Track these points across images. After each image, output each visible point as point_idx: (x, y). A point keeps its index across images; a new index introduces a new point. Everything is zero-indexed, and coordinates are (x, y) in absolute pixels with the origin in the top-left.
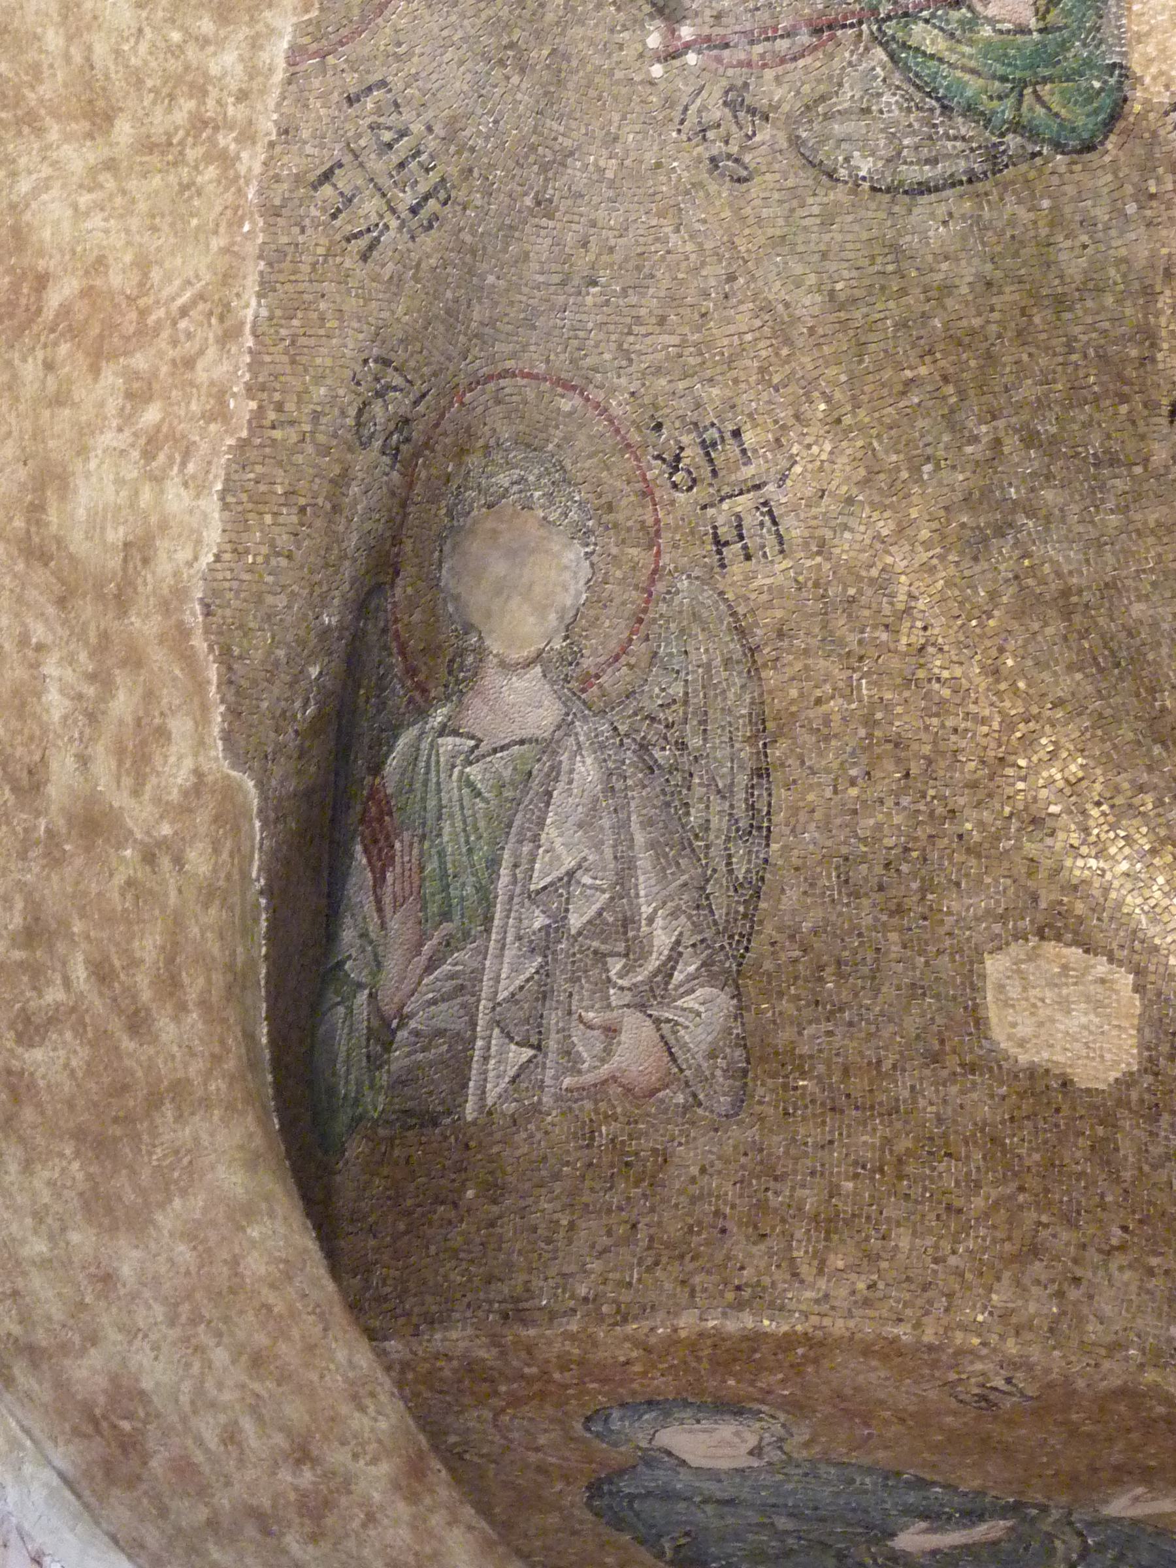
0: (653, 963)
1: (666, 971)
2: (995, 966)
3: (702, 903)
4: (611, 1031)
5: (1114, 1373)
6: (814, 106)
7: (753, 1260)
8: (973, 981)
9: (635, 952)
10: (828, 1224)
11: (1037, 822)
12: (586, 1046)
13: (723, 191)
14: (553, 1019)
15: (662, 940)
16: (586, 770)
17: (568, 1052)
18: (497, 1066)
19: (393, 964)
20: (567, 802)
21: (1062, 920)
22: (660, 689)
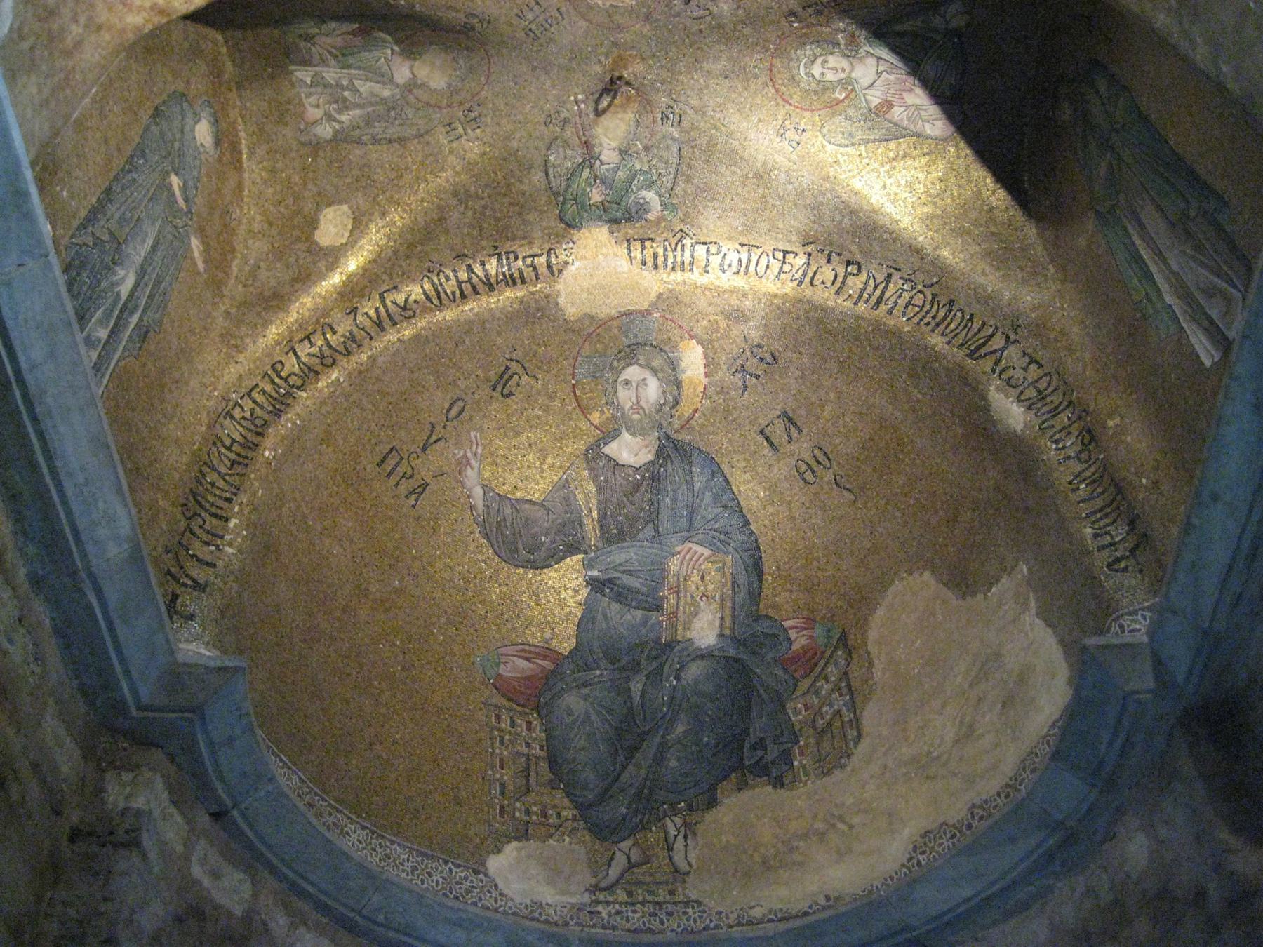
0: (337, 117)
1: (335, 120)
2: (345, 207)
3: (355, 128)
4: (318, 106)
5: (239, 247)
6: (566, 144)
7: (261, 151)
8: (340, 202)
9: (339, 111)
10: (273, 171)
11: (383, 215)
12: (313, 100)
13: (542, 118)
14: (319, 90)
15: (344, 118)
16: (386, 93)
17: (311, 94)
18: (303, 75)
19: (329, 40)
20: (377, 88)
21: (359, 224)
22: (410, 112)
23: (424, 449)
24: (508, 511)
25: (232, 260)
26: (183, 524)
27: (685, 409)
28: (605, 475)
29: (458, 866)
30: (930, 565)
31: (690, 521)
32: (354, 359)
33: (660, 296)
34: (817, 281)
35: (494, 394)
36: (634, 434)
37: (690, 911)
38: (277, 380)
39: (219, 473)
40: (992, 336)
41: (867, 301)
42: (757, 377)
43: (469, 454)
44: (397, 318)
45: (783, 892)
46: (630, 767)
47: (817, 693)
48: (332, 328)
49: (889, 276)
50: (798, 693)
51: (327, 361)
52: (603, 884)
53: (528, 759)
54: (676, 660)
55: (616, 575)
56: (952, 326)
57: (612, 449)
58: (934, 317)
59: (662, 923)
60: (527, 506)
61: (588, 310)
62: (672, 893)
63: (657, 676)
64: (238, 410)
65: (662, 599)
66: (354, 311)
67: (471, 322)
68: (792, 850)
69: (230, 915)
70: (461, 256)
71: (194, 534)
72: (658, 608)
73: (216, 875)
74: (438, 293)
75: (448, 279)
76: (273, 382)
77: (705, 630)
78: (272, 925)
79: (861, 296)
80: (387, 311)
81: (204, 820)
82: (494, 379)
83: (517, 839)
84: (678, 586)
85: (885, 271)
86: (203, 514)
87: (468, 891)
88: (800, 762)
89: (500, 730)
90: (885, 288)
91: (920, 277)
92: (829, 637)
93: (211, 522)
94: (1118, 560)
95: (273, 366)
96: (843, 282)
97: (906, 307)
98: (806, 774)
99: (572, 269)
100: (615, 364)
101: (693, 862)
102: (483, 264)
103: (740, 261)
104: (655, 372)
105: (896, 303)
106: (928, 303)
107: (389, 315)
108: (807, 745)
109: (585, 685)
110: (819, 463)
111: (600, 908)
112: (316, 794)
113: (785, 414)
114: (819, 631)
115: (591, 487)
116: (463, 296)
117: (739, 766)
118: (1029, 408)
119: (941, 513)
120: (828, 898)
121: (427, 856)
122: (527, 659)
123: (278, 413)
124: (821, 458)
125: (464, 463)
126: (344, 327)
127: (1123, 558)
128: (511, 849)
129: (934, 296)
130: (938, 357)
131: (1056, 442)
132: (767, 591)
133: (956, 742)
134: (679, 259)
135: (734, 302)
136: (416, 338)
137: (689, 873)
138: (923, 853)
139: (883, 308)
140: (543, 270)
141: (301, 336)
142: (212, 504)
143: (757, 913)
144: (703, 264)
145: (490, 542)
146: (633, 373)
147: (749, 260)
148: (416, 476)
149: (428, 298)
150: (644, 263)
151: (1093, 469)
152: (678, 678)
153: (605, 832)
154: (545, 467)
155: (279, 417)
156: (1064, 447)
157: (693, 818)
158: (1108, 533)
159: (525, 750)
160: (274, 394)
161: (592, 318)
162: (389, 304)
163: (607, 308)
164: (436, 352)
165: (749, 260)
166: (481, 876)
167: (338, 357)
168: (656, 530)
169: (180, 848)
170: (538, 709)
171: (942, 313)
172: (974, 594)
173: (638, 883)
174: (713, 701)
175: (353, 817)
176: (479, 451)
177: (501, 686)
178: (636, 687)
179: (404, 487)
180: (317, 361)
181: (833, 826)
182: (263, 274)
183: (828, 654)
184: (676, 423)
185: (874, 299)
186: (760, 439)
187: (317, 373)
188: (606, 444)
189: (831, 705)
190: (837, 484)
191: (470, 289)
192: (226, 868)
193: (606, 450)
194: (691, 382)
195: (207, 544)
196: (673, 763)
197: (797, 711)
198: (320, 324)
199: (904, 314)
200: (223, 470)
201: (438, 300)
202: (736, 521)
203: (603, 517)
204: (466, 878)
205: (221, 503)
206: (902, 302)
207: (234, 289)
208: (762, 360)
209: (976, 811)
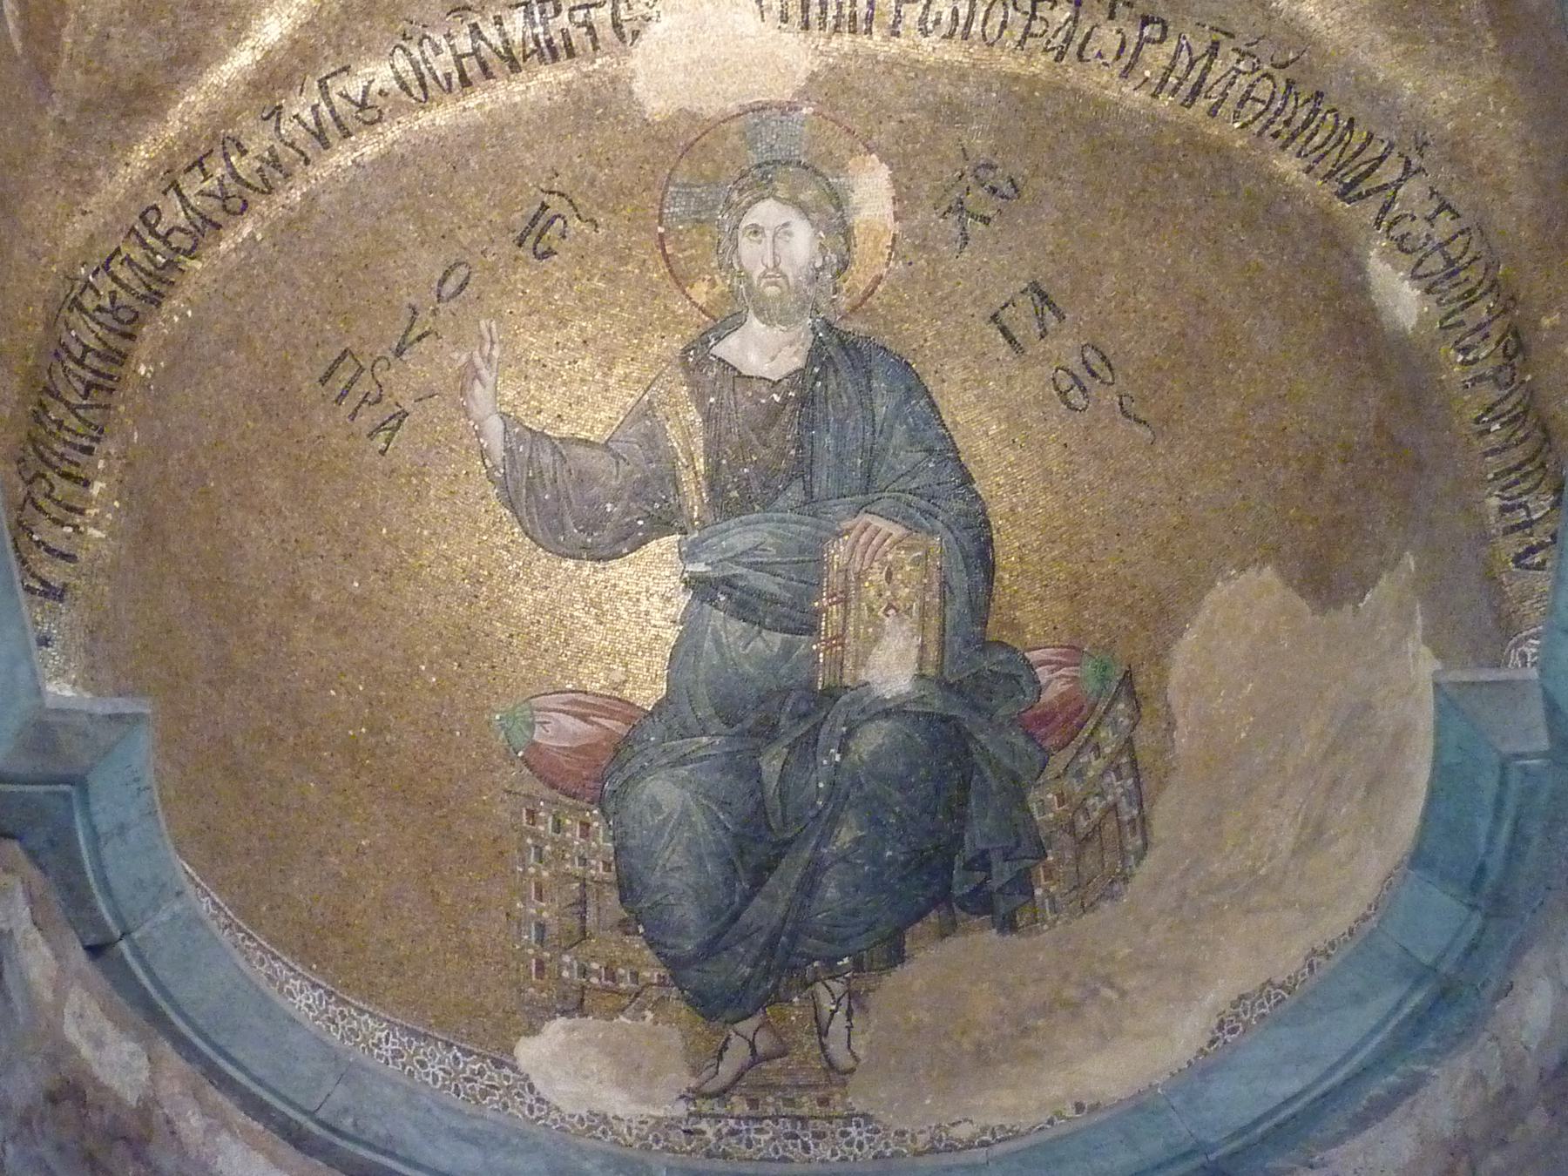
23: (399, 352)
24: (547, 459)
25: (63, 26)
26: (21, 491)
27: (859, 278)
28: (718, 393)
29: (469, 1053)
30: (1273, 554)
31: (869, 476)
32: (279, 199)
33: (813, 77)
34: (1089, 54)
35: (521, 253)
36: (769, 321)
37: (853, 1130)
38: (150, 240)
39: (67, 404)
40: (1382, 159)
41: (1175, 91)
42: (986, 220)
43: (478, 361)
44: (351, 124)
45: (1008, 1099)
46: (758, 901)
47: (1080, 774)
48: (239, 145)
49: (1215, 46)
50: (1049, 774)
51: (234, 204)
52: (710, 1087)
53: (584, 885)
54: (841, 719)
55: (739, 570)
56: (1317, 140)
57: (729, 348)
58: (1287, 123)
59: (806, 1148)
60: (580, 450)
61: (686, 104)
62: (824, 1102)
63: (807, 747)
64: (89, 294)
65: (817, 613)
66: (277, 111)
67: (479, 128)
68: (1026, 1032)
69: (119, 1102)
70: (461, 10)
71: (39, 508)
72: (811, 629)
73: (98, 1043)
74: (421, 78)
75: (437, 50)
76: (144, 244)
77: (892, 666)
78: (181, 1125)
79: (1164, 81)
80: (332, 111)
81: (78, 956)
82: (521, 226)
83: (564, 1013)
84: (845, 592)
85: (1208, 37)
86: (49, 473)
87: (484, 1094)
88: (1046, 891)
89: (535, 836)
90: (1207, 68)
91: (1265, 50)
92: (1104, 680)
93: (63, 488)
94: (1531, 550)
95: (143, 217)
96: (1136, 55)
97: (1241, 104)
98: (1055, 911)
99: (654, 27)
100: (735, 197)
101: (861, 1053)
102: (498, 21)
103: (955, 12)
104: (804, 210)
105: (1224, 94)
106: (1279, 95)
107: (336, 119)
108: (1059, 861)
109: (683, 760)
110: (1094, 374)
111: (703, 1125)
112: (240, 929)
113: (1035, 288)
114: (1088, 668)
115: (693, 416)
116: (465, 82)
117: (943, 898)
118: (1428, 291)
119: (1294, 465)
120: (1079, 1107)
121: (417, 1035)
122: (584, 718)
123: (155, 299)
124: (1097, 364)
125: (469, 374)
126: (260, 141)
127: (1542, 546)
128: (556, 1029)
129: (1290, 84)
130: (1291, 195)
131: (1465, 351)
132: (1001, 599)
133: (1294, 853)
134: (847, 11)
135: (944, 88)
136: (385, 158)
137: (852, 1071)
138: (1233, 1031)
139: (1203, 103)
140: (606, 33)
141: (186, 161)
142: (62, 457)
143: (963, 1132)
144: (890, 20)
145: (515, 513)
146: (767, 212)
147: (972, 14)
148: (386, 400)
149: (404, 87)
150: (785, 18)
151: (1514, 399)
152: (844, 750)
153: (716, 1006)
154: (612, 381)
155: (159, 305)
156: (1476, 360)
157: (860, 985)
158: (1523, 506)
159: (578, 869)
160: (146, 264)
161: (693, 116)
162: (336, 98)
163: (718, 98)
164: (417, 179)
165: (972, 14)
166: (506, 1071)
167: (251, 196)
168: (809, 493)
169: (48, 996)
170: (600, 802)
171: (1303, 115)
172: (1338, 604)
173: (769, 1087)
174: (902, 789)
175: (298, 968)
176: (496, 353)
177: (538, 762)
178: (772, 764)
179: (367, 419)
180: (217, 203)
181: (1095, 993)
182: (116, 49)
183: (1101, 707)
184: (844, 302)
185: (1186, 88)
186: (993, 331)
187: (218, 226)
188: (719, 339)
189: (1102, 795)
190: (1125, 413)
191: (477, 69)
192: (110, 1032)
193: (720, 350)
194: (869, 229)
195: (60, 523)
196: (832, 893)
197: (1045, 805)
198: (221, 137)
199: (1236, 118)
200: (74, 399)
201: (422, 89)
202: (949, 475)
203: (714, 469)
204: (481, 1073)
205: (75, 456)
206: (1235, 93)
207: (71, 79)
208: (994, 190)
209: (1316, 960)
